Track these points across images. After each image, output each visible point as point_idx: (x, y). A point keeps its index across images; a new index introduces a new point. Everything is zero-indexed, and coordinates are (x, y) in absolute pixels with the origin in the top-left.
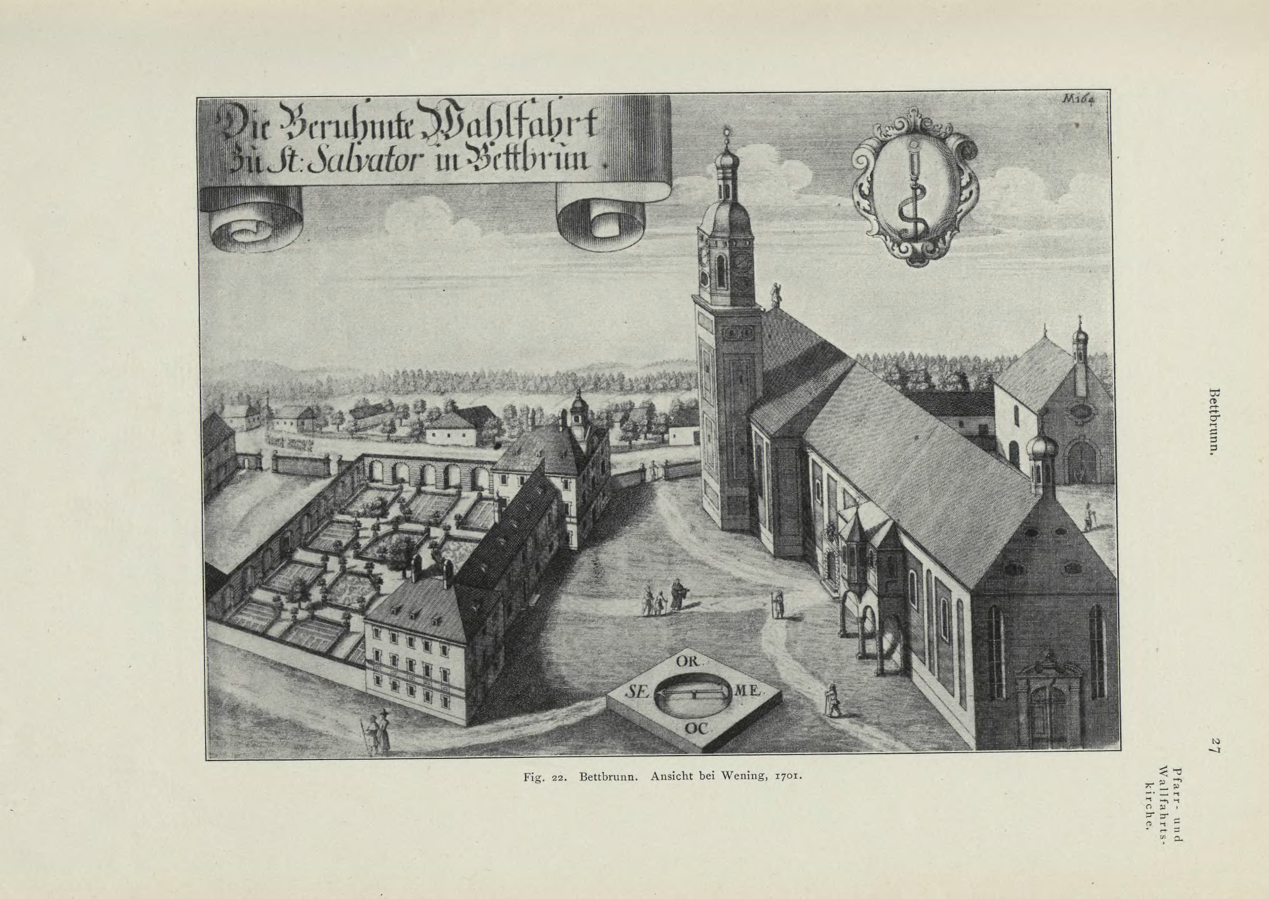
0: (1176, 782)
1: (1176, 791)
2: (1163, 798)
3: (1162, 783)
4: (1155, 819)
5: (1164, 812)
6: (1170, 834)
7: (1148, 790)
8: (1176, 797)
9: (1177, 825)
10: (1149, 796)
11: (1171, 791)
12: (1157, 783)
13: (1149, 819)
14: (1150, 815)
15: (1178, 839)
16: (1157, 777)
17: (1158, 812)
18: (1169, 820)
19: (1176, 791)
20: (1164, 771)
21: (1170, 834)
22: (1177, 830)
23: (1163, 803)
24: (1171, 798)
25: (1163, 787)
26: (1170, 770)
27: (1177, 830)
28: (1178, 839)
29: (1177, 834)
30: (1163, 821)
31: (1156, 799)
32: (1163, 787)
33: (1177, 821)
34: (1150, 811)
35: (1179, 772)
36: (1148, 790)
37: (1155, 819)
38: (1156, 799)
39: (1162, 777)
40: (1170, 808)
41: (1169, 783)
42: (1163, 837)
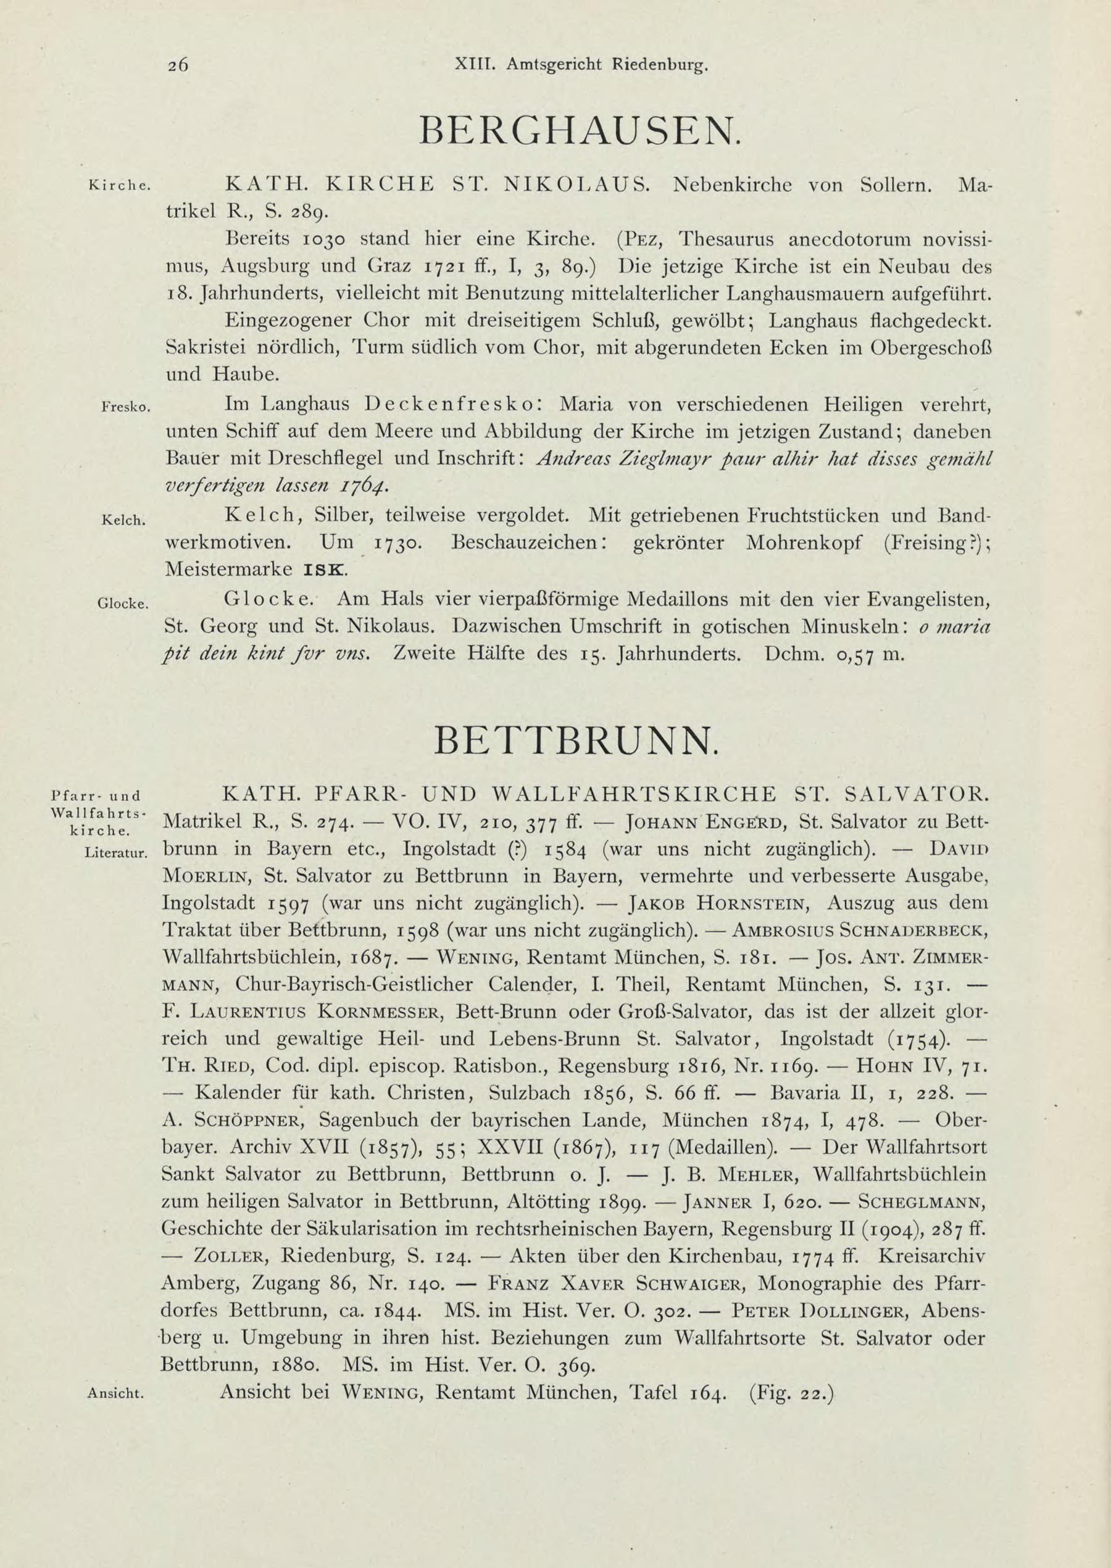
0: (69, 797)
1: (79, 797)
2: (88, 814)
3: (70, 815)
5: (106, 814)
6: (132, 806)
8: (87, 798)
9: (119, 797)
11: (79, 803)
15: (137, 796)
16: (64, 822)
18: (117, 807)
19: (79, 797)
20: (57, 812)
21: (132, 806)
22: (125, 797)
23: (95, 814)
26: (55, 804)
27: (125, 797)
28: (137, 796)
29: (130, 797)
30: (117, 815)
31: (90, 823)
32: (74, 814)
33: (113, 798)
35: (56, 793)
38: (90, 823)
40: (102, 805)
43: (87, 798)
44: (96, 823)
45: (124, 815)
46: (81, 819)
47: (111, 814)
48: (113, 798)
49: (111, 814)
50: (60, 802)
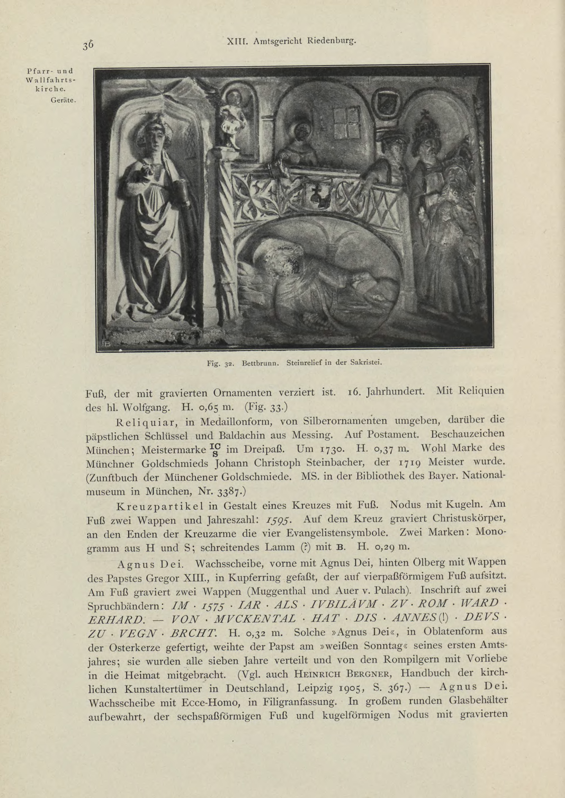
0: (36, 72)
1: (42, 72)
2: (46, 81)
4: (58, 85)
5: (55, 80)
6: (69, 76)
7: (40, 90)
8: (46, 72)
9: (62, 72)
10: (44, 90)
11: (42, 75)
12: (36, 84)
13: (59, 90)
14: (56, 90)
15: (71, 71)
16: (33, 84)
17: (55, 84)
18: (60, 76)
19: (42, 72)
20: (29, 80)
21: (69, 76)
22: (65, 72)
23: (49, 81)
24: (46, 76)
25: (39, 81)
26: (29, 76)
27: (65, 72)
29: (68, 72)
32: (39, 81)
33: (59, 72)
34: (53, 89)
36: (40, 90)
37: (58, 85)
39: (33, 81)
40: (52, 76)
41: (37, 76)
42: (70, 80)
43: (46, 72)
44: (49, 85)
45: (64, 81)
46: (43, 84)
47: (57, 80)
48: (59, 72)
49: (57, 80)
50: (31, 75)
